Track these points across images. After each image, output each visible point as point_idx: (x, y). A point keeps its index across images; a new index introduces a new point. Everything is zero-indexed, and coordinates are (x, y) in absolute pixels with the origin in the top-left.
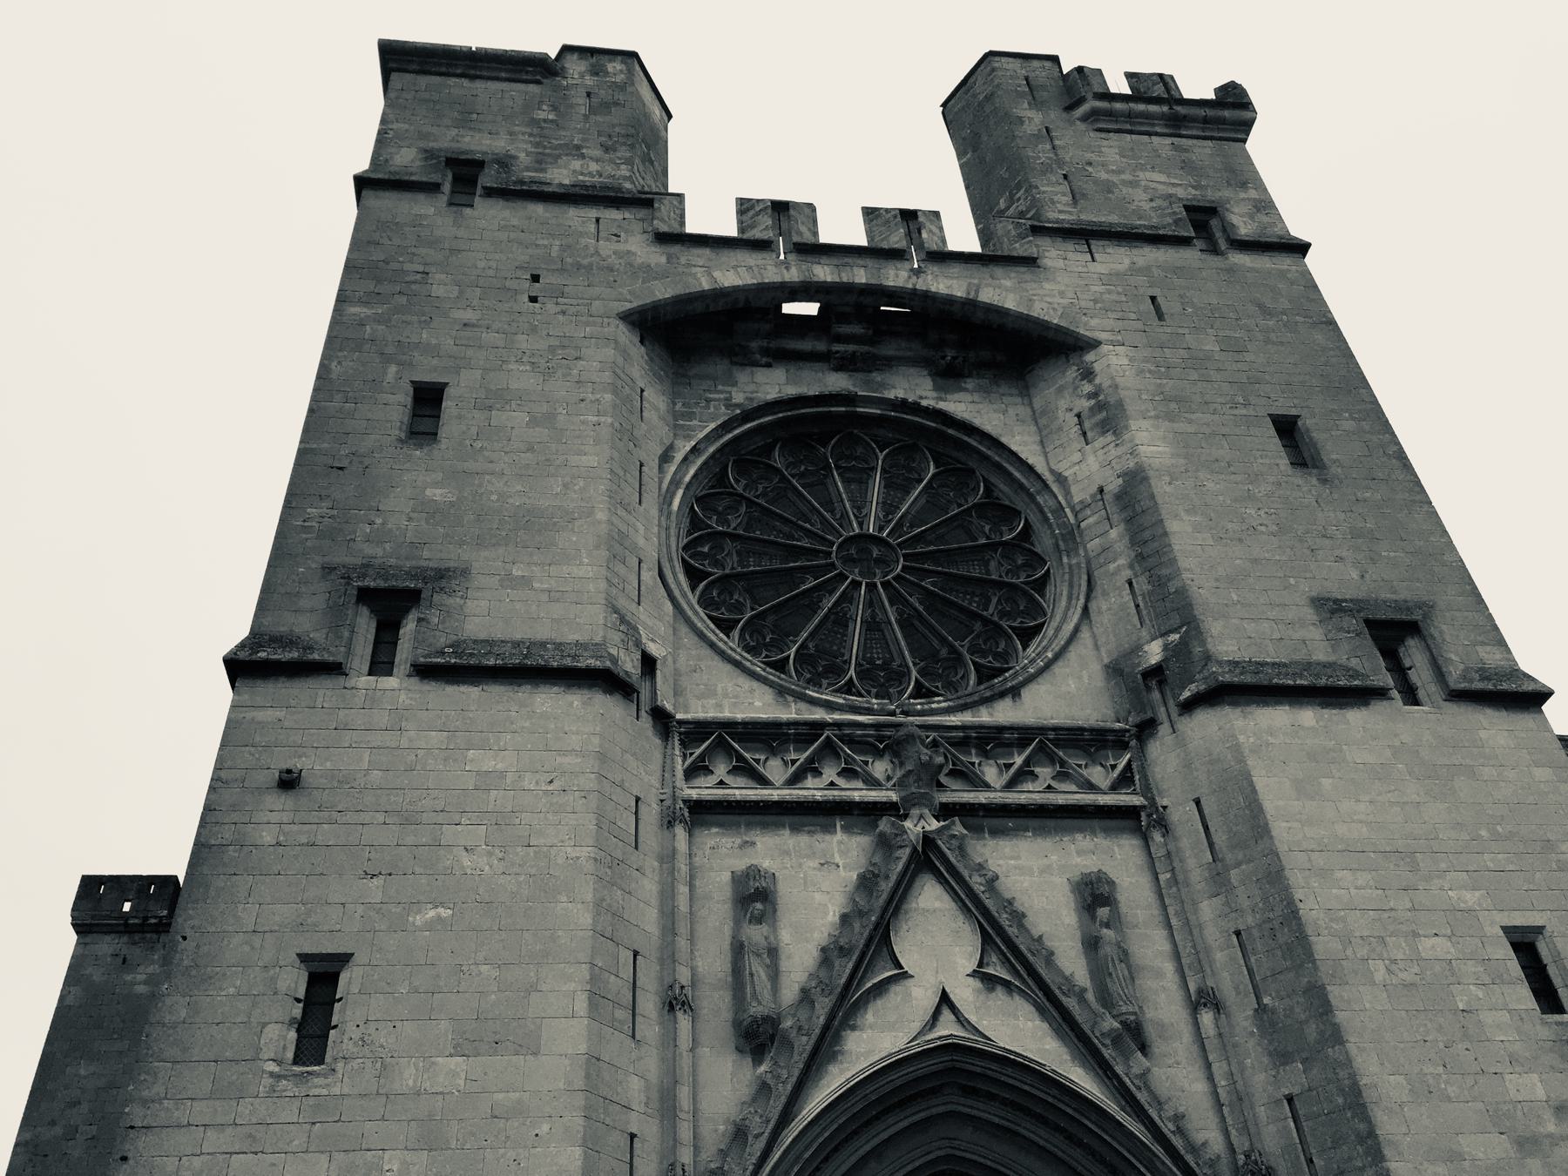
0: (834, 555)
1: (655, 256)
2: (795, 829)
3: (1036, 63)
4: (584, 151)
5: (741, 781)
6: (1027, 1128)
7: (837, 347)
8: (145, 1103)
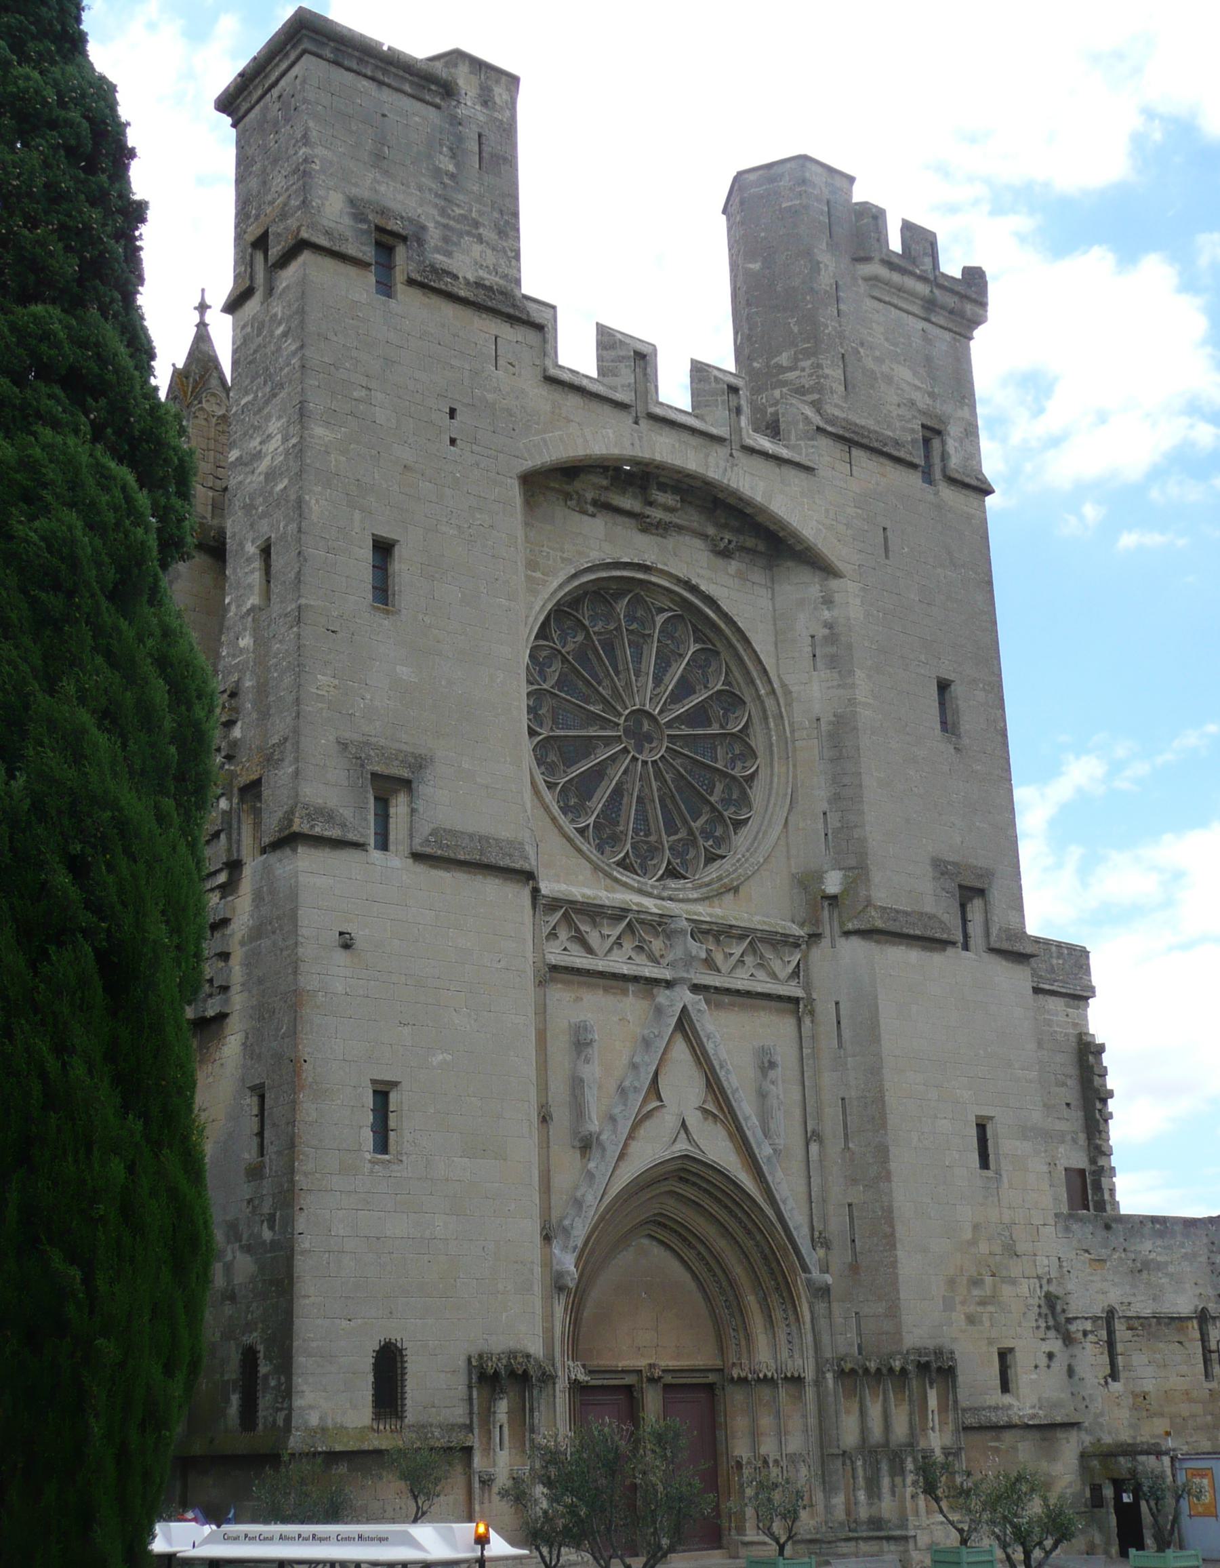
0: (621, 728)
1: (540, 397)
2: (606, 990)
3: (837, 178)
4: (481, 230)
5: (575, 948)
6: (707, 1203)
7: (649, 511)
8: (306, 1174)
